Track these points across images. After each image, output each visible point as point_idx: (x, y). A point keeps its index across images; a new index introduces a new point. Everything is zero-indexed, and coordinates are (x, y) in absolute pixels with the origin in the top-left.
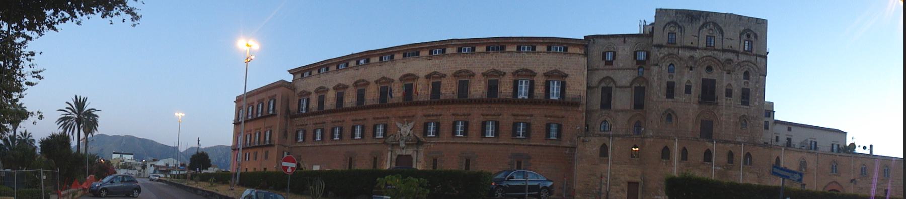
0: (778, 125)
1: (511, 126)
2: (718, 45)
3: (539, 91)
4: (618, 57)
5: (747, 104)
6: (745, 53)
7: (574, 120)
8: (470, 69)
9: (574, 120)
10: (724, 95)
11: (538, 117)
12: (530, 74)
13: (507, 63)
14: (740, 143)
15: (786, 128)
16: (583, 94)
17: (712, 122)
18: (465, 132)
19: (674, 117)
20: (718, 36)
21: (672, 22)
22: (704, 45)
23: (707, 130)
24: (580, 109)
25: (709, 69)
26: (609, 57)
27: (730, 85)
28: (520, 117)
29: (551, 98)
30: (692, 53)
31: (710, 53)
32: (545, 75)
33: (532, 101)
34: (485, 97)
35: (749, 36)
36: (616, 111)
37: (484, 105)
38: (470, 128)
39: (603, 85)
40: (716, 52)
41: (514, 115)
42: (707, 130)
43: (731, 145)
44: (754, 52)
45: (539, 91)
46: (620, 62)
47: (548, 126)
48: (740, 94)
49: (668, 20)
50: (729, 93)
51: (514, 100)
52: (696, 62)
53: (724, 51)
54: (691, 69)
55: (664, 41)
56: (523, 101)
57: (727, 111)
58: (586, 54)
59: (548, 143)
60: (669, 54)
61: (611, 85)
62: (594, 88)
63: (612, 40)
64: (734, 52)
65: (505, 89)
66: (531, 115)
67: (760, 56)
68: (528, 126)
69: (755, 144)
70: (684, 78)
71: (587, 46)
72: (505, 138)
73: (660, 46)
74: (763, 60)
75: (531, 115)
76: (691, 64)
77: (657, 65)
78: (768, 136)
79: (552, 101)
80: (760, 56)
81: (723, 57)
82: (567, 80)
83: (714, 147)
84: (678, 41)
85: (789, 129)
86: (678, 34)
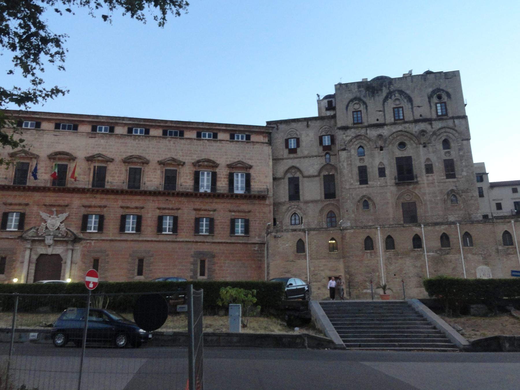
0: (496, 190)
1: (192, 222)
2: (409, 117)
3: (222, 185)
4: (303, 144)
5: (453, 176)
6: (440, 118)
8: (144, 155)
10: (424, 171)
12: (212, 165)
13: (187, 151)
14: (454, 223)
15: (509, 190)
16: (270, 186)
17: (414, 203)
18: (138, 228)
19: (370, 202)
21: (355, 99)
22: (392, 120)
23: (410, 214)
24: (267, 202)
25: (402, 145)
26: (292, 144)
27: (428, 159)
28: (202, 212)
29: (236, 192)
30: (380, 131)
31: (400, 128)
32: (230, 166)
33: (214, 194)
34: (161, 189)
35: (439, 97)
36: (306, 202)
37: (161, 198)
38: (144, 223)
39: (289, 175)
40: (407, 125)
41: (195, 210)
42: (410, 214)
43: (443, 227)
44: (450, 115)
45: (222, 185)
46: (304, 150)
47: (233, 222)
49: (351, 96)
50: (429, 169)
51: (195, 194)
52: (385, 141)
53: (416, 121)
54: (381, 150)
55: (349, 122)
56: (205, 195)
57: (430, 188)
58: (270, 143)
59: (233, 240)
60: (357, 137)
61: (298, 175)
62: (280, 179)
63: (294, 125)
64: (429, 121)
65: (185, 181)
66: (215, 210)
67: (459, 117)
68: (211, 222)
69: (472, 222)
70: (375, 160)
72: (185, 234)
73: (345, 128)
74: (463, 121)
75: (215, 210)
76: (380, 143)
77: (344, 149)
78: (486, 207)
79: (237, 196)
80: (459, 117)
81: (415, 129)
82: (251, 172)
83: (422, 231)
84: (364, 120)
85: (515, 191)
86: (364, 111)
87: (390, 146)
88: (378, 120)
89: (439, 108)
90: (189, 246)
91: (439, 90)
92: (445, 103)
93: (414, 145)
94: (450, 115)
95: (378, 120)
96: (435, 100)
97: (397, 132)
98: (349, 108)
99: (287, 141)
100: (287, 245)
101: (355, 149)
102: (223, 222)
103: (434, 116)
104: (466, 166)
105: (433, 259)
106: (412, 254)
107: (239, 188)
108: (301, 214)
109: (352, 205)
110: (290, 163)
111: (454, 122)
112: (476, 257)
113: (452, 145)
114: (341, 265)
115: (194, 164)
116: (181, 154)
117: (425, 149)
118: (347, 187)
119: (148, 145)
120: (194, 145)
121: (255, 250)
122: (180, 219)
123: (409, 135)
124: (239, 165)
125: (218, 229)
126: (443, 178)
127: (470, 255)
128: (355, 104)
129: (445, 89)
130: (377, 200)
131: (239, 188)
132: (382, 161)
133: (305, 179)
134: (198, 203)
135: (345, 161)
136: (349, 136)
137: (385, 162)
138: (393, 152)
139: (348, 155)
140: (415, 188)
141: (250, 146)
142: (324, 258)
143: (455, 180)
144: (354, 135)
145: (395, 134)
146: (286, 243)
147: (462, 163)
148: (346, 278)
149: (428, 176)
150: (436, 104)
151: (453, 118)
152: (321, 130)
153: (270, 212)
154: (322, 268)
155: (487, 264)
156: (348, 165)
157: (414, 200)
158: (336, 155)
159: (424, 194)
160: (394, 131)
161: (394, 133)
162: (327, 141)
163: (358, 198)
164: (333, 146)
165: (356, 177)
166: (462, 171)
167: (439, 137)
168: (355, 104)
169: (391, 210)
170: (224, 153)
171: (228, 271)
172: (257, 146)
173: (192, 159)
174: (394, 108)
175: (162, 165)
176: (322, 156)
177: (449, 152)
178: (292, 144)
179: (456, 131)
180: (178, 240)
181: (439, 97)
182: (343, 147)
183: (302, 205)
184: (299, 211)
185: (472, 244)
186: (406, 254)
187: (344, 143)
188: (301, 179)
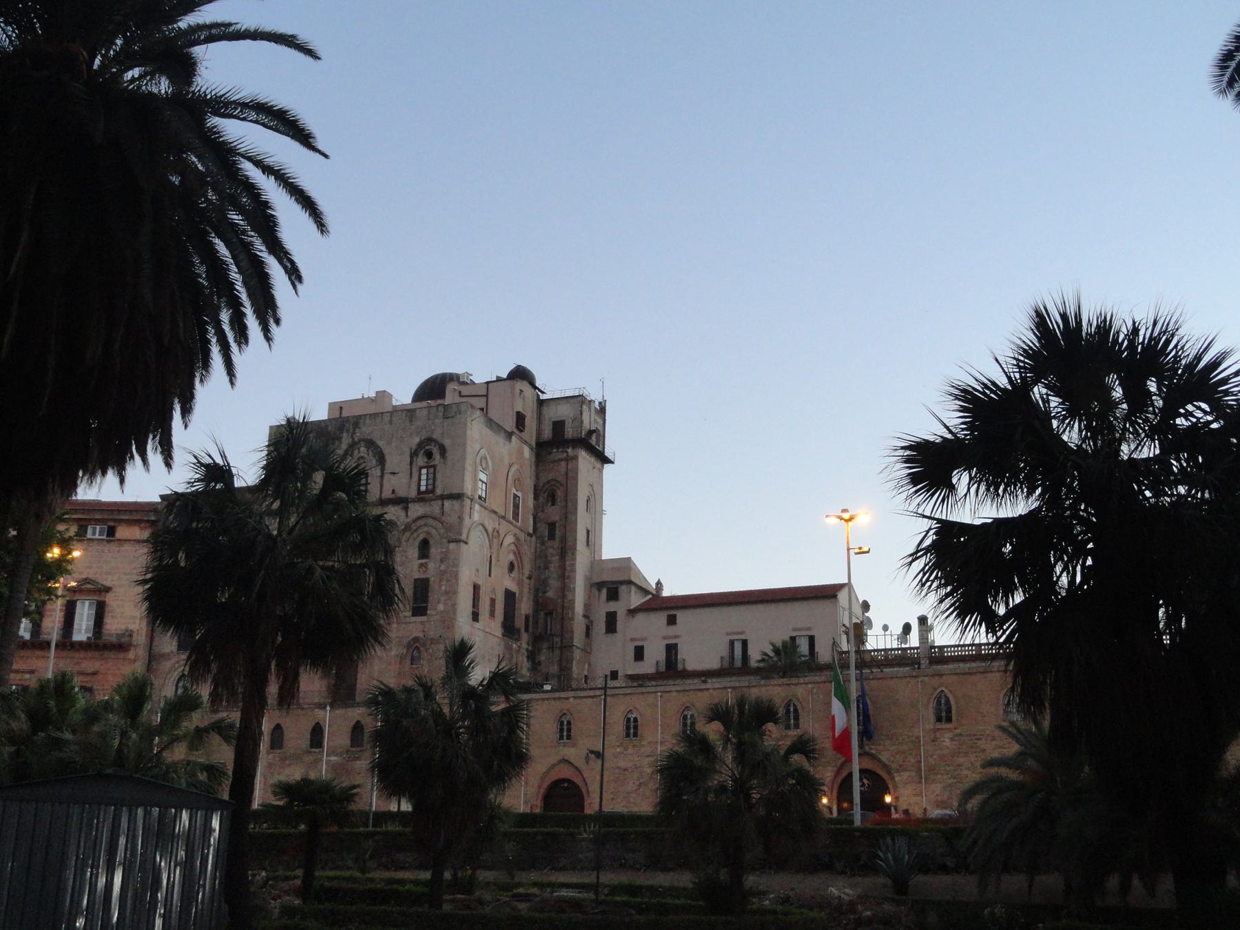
6: (422, 497)
44: (439, 492)
64: (403, 502)
82: (109, 598)
89: (424, 477)
91: (430, 440)
92: (434, 467)
94: (439, 492)
96: (421, 460)
104: (447, 593)
113: (433, 550)
124: (89, 586)
129: (439, 439)
131: (82, 632)
141: (114, 547)
150: (421, 468)
151: (443, 498)
167: (415, 535)
172: (127, 547)
181: (429, 455)
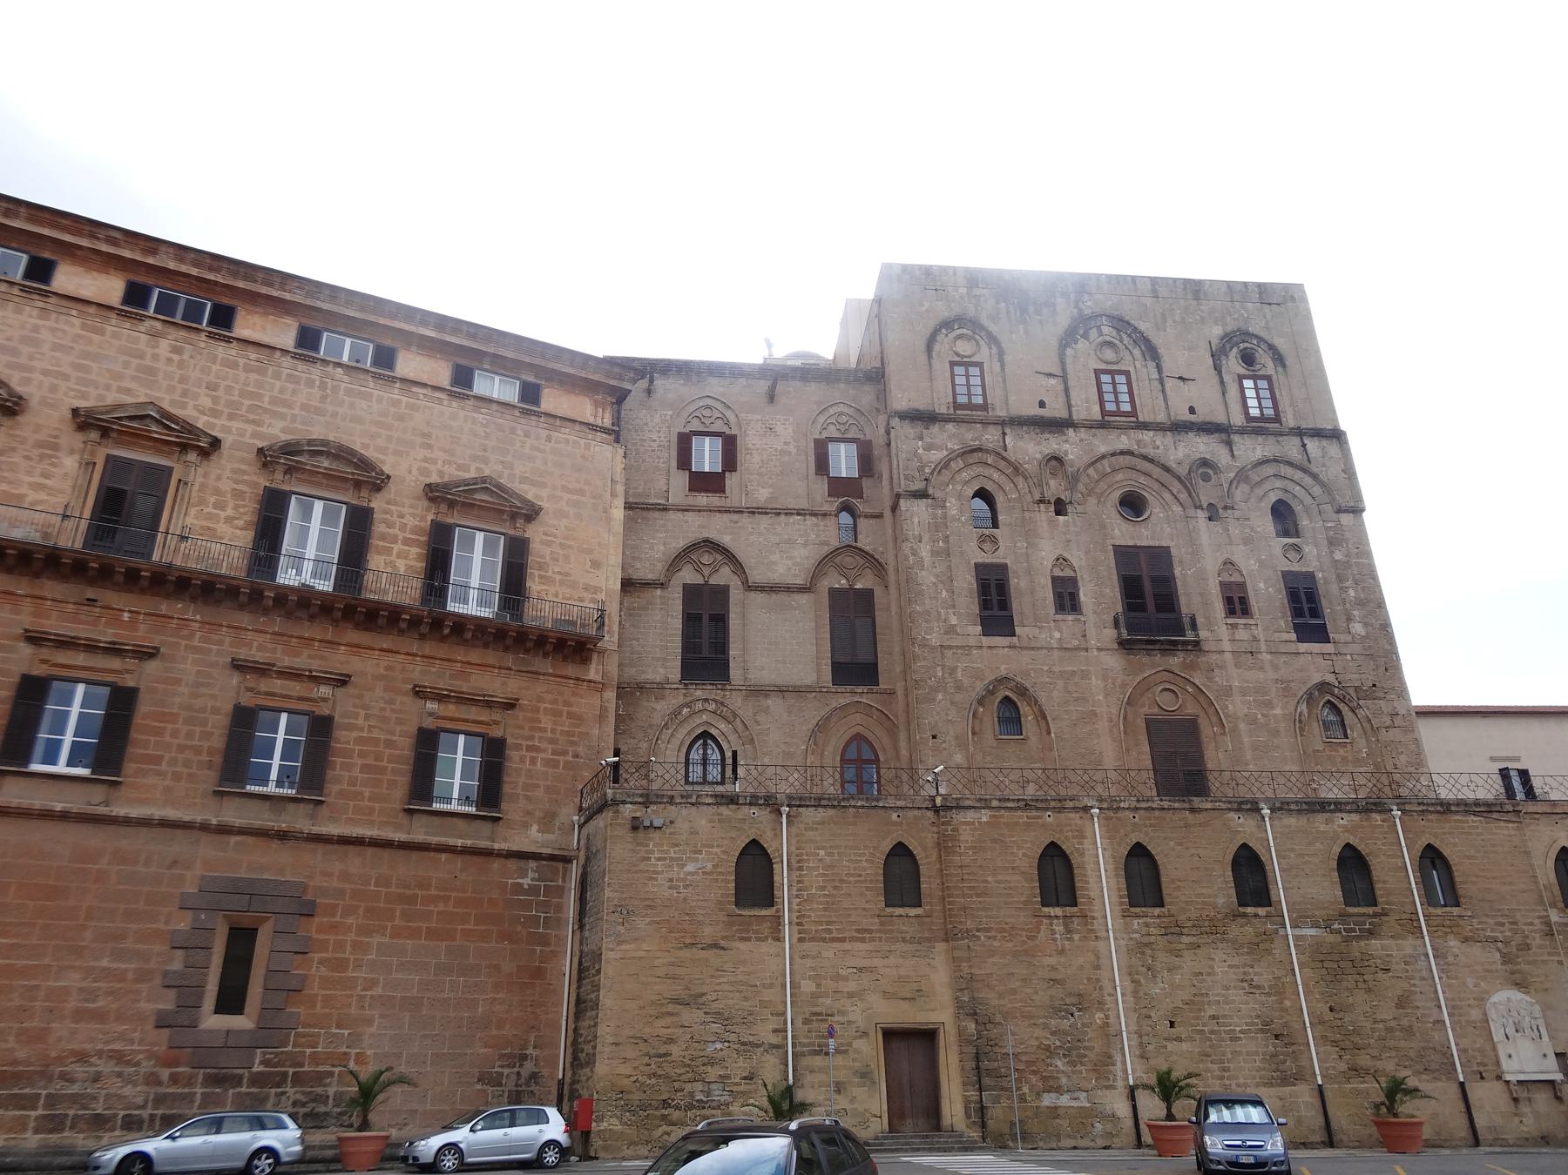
3: (394, 571)
6: (1258, 427)
7: (561, 728)
9: (561, 728)
10: (1219, 607)
11: (378, 697)
12: (358, 477)
20: (1143, 372)
22: (1096, 412)
23: (1179, 765)
24: (593, 672)
25: (1133, 505)
27: (1229, 563)
28: (278, 685)
29: (453, 607)
30: (1052, 444)
31: (1124, 441)
32: (436, 494)
33: (349, 608)
37: (52, 588)
40: (1147, 436)
41: (238, 666)
42: (1179, 765)
44: (1290, 421)
45: (394, 571)
47: (427, 746)
48: (1280, 598)
50: (1237, 603)
51: (251, 592)
52: (1073, 481)
53: (1178, 428)
54: (1060, 508)
56: (303, 603)
59: (420, 832)
60: (970, 452)
66: (342, 681)
67: (1318, 433)
70: (1037, 550)
71: (620, 397)
73: (925, 418)
74: (1333, 449)
75: (342, 681)
76: (1055, 488)
77: (922, 495)
79: (461, 625)
80: (1318, 433)
87: (1092, 501)
88: (1042, 404)
90: (178, 845)
91: (1246, 335)
92: (1268, 378)
93: (1178, 509)
94: (1290, 421)
95: (1042, 404)
96: (1233, 364)
97: (1113, 455)
98: (937, 347)
99: (684, 444)
100: (690, 867)
101: (960, 497)
102: (375, 742)
103: (1238, 419)
104: (1361, 603)
105: (1318, 956)
106: (1234, 930)
107: (474, 590)
108: (732, 738)
109: (952, 715)
110: (694, 527)
111: (1304, 446)
112: (1476, 951)
113: (1304, 522)
114: (938, 974)
115: (266, 458)
116: (206, 402)
117: (1216, 527)
118: (935, 639)
119: (36, 329)
120: (277, 376)
121: (518, 888)
122: (144, 707)
123: (1156, 471)
125: (343, 774)
126: (1285, 636)
127: (1453, 943)
128: (959, 337)
129: (1262, 334)
130: (1051, 698)
132: (1066, 555)
133: (759, 598)
134: (259, 641)
135: (926, 538)
136: (939, 448)
137: (1077, 558)
138: (1103, 526)
139: (934, 516)
140: (1192, 666)
142: (862, 935)
143: (1329, 648)
144: (955, 446)
145: (1105, 462)
146: (687, 858)
147: (1343, 589)
148: (961, 1032)
149: (1234, 626)
150: (1241, 378)
151: (1299, 432)
152: (821, 419)
153: (602, 717)
154: (852, 986)
155: (1521, 985)
156: (934, 553)
157: (1191, 709)
158: (880, 516)
159: (1228, 691)
160: (1103, 449)
161: (1103, 457)
162: (844, 462)
163: (980, 687)
164: (866, 483)
165: (968, 603)
166: (1349, 619)
167: (1259, 491)
168: (959, 337)
169: (1107, 750)
170: (419, 438)
171: (378, 991)
172: (566, 434)
173: (255, 435)
174: (1098, 373)
175: (94, 435)
176: (825, 515)
177: (1297, 548)
178: (707, 456)
179: (1315, 477)
180: (119, 810)
181: (1248, 359)
182: (918, 485)
183: (735, 701)
184: (723, 726)
185: (1454, 898)
186: (1212, 929)
187: (920, 469)
188: (736, 594)
